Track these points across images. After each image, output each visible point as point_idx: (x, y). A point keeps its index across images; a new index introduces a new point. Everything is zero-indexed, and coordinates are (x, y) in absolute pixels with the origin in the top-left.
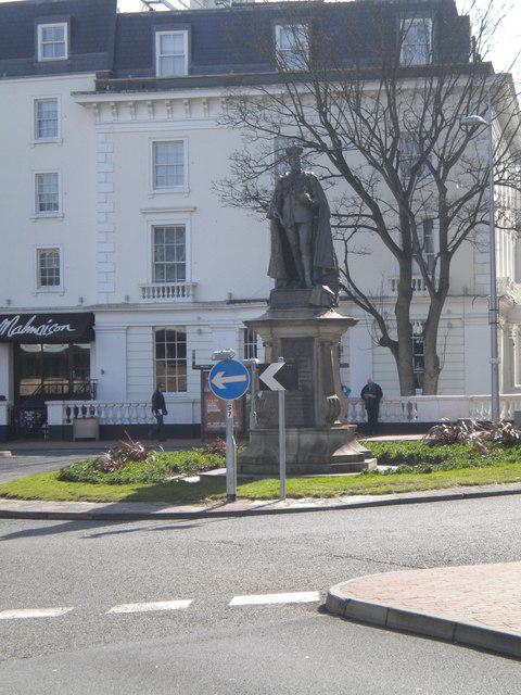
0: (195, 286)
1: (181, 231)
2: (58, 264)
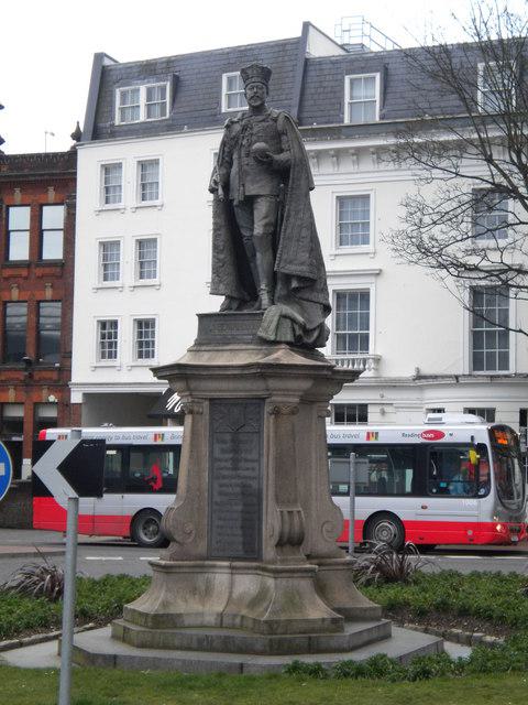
0: (378, 360)
1: (364, 297)
2: (153, 337)
